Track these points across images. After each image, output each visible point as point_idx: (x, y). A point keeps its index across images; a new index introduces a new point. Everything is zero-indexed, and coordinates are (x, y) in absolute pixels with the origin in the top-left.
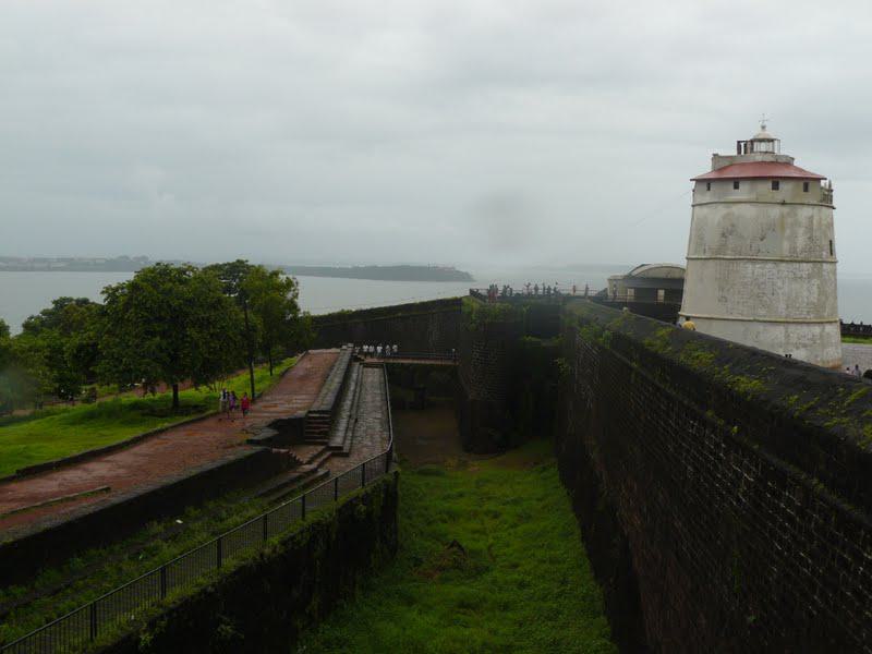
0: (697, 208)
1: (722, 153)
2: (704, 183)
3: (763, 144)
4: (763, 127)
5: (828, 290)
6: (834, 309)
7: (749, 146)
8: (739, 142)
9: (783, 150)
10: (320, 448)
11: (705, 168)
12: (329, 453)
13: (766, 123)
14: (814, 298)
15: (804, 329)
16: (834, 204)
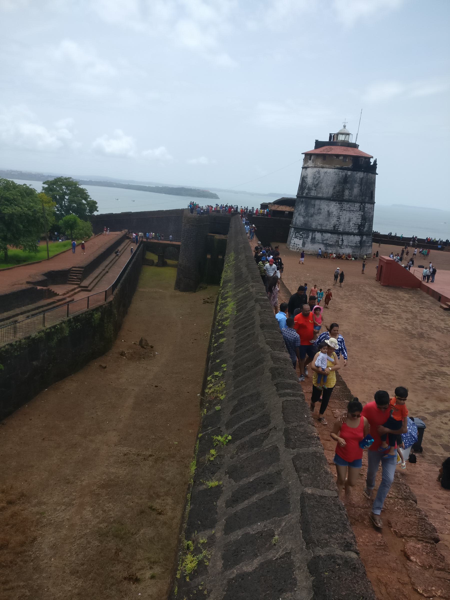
0: (304, 170)
1: (320, 140)
2: (308, 156)
3: (344, 136)
4: (345, 127)
5: (367, 219)
6: (371, 226)
7: (335, 137)
8: (330, 134)
9: (352, 140)
10: (76, 286)
11: (311, 147)
12: (79, 289)
13: (346, 124)
15: (352, 238)
16: (377, 172)
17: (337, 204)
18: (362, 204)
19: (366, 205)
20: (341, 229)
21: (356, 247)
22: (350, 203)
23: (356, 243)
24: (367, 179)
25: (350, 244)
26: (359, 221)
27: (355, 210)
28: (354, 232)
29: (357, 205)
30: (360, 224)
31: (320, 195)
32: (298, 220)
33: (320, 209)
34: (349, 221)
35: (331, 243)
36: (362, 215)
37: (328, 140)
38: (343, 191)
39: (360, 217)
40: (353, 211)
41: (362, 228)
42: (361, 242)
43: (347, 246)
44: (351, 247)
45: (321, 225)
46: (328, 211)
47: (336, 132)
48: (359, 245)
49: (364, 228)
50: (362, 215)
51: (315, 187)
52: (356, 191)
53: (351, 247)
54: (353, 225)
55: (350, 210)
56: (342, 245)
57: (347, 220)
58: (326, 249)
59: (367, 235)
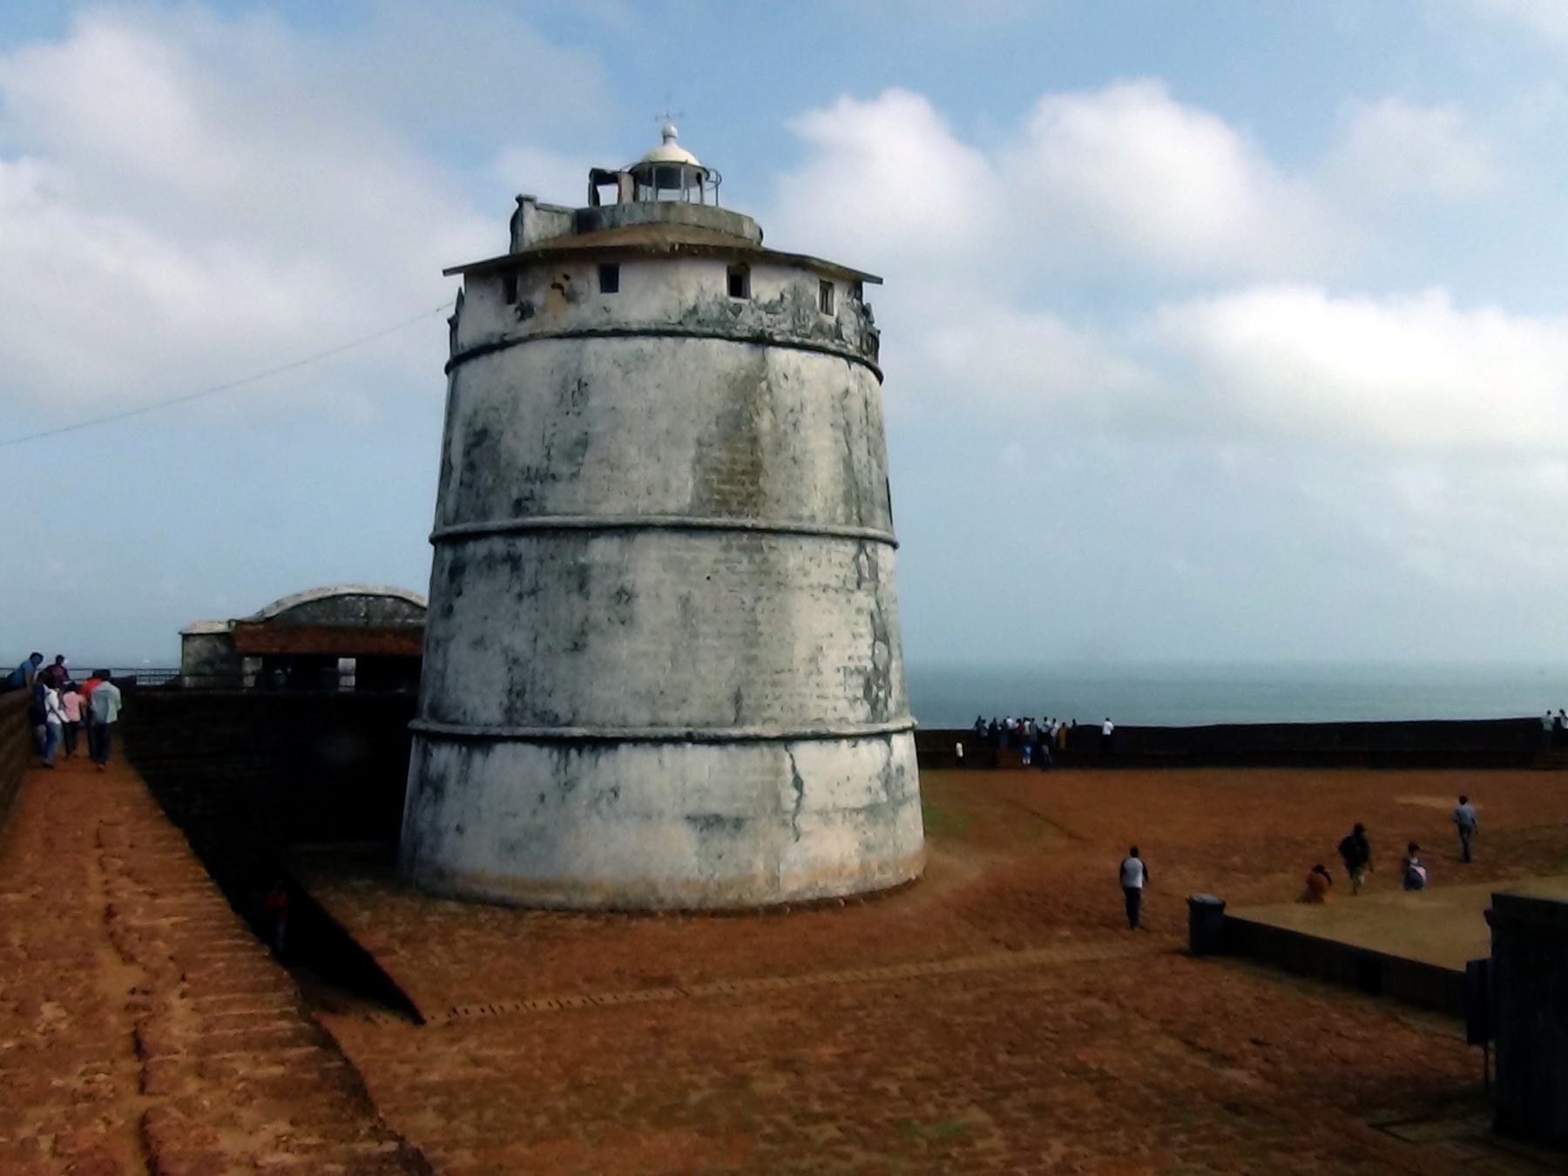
0: (473, 371)
17: (735, 554)
18: (862, 548)
21: (872, 810)
22: (808, 544)
23: (869, 789)
25: (843, 803)
26: (864, 647)
27: (834, 583)
28: (851, 716)
30: (870, 666)
31: (612, 509)
32: (471, 682)
33: (624, 596)
40: (825, 589)
41: (882, 694)
46: (685, 602)
51: (570, 457)
54: (840, 676)
55: (811, 586)
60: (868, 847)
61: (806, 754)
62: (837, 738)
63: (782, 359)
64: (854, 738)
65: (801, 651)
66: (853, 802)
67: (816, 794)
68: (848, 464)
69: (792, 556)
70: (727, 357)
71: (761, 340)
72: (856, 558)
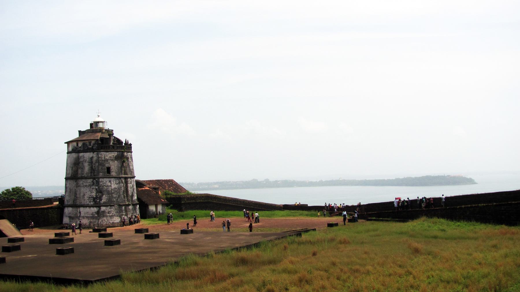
1: (83, 129)
4: (98, 116)
14: (94, 194)
15: (87, 209)
19: (101, 180)
20: (78, 203)
21: (93, 217)
22: (83, 180)
24: (98, 157)
29: (90, 181)
34: (84, 195)
35: (72, 216)
36: (96, 189)
37: (89, 128)
38: (77, 171)
39: (94, 191)
40: (86, 186)
42: (98, 213)
43: (83, 217)
44: (87, 217)
45: (67, 201)
47: (92, 121)
48: (96, 215)
49: (101, 200)
50: (96, 189)
52: (87, 168)
53: (87, 217)
56: (80, 216)
57: (82, 194)
58: (70, 222)
59: (104, 206)
60: (91, 222)
61: (82, 209)
62: (86, 207)
63: (81, 154)
64: (90, 207)
65: (82, 194)
66: (88, 216)
67: (82, 215)
68: (92, 167)
69: (81, 182)
70: (74, 155)
71: (79, 152)
72: (93, 181)
